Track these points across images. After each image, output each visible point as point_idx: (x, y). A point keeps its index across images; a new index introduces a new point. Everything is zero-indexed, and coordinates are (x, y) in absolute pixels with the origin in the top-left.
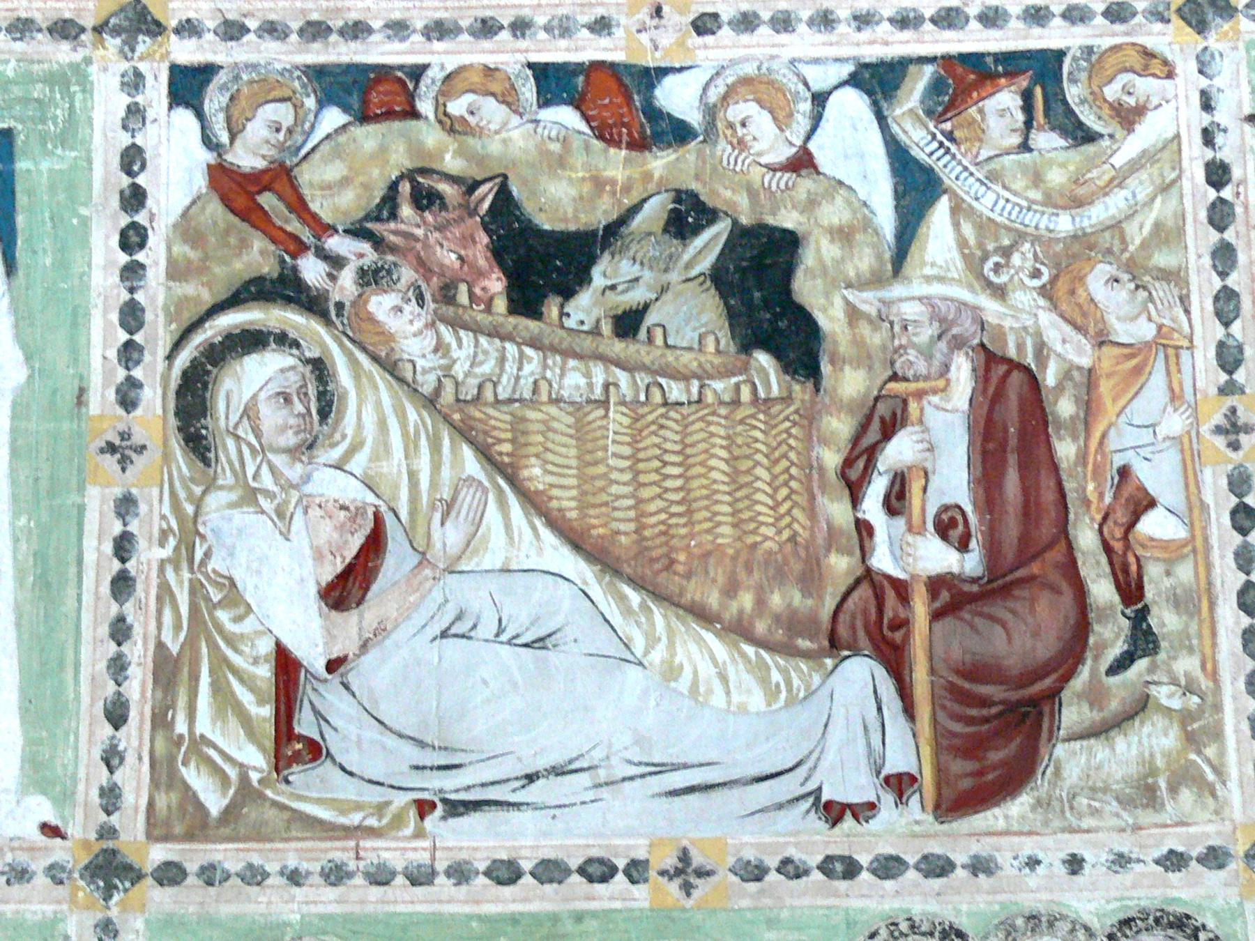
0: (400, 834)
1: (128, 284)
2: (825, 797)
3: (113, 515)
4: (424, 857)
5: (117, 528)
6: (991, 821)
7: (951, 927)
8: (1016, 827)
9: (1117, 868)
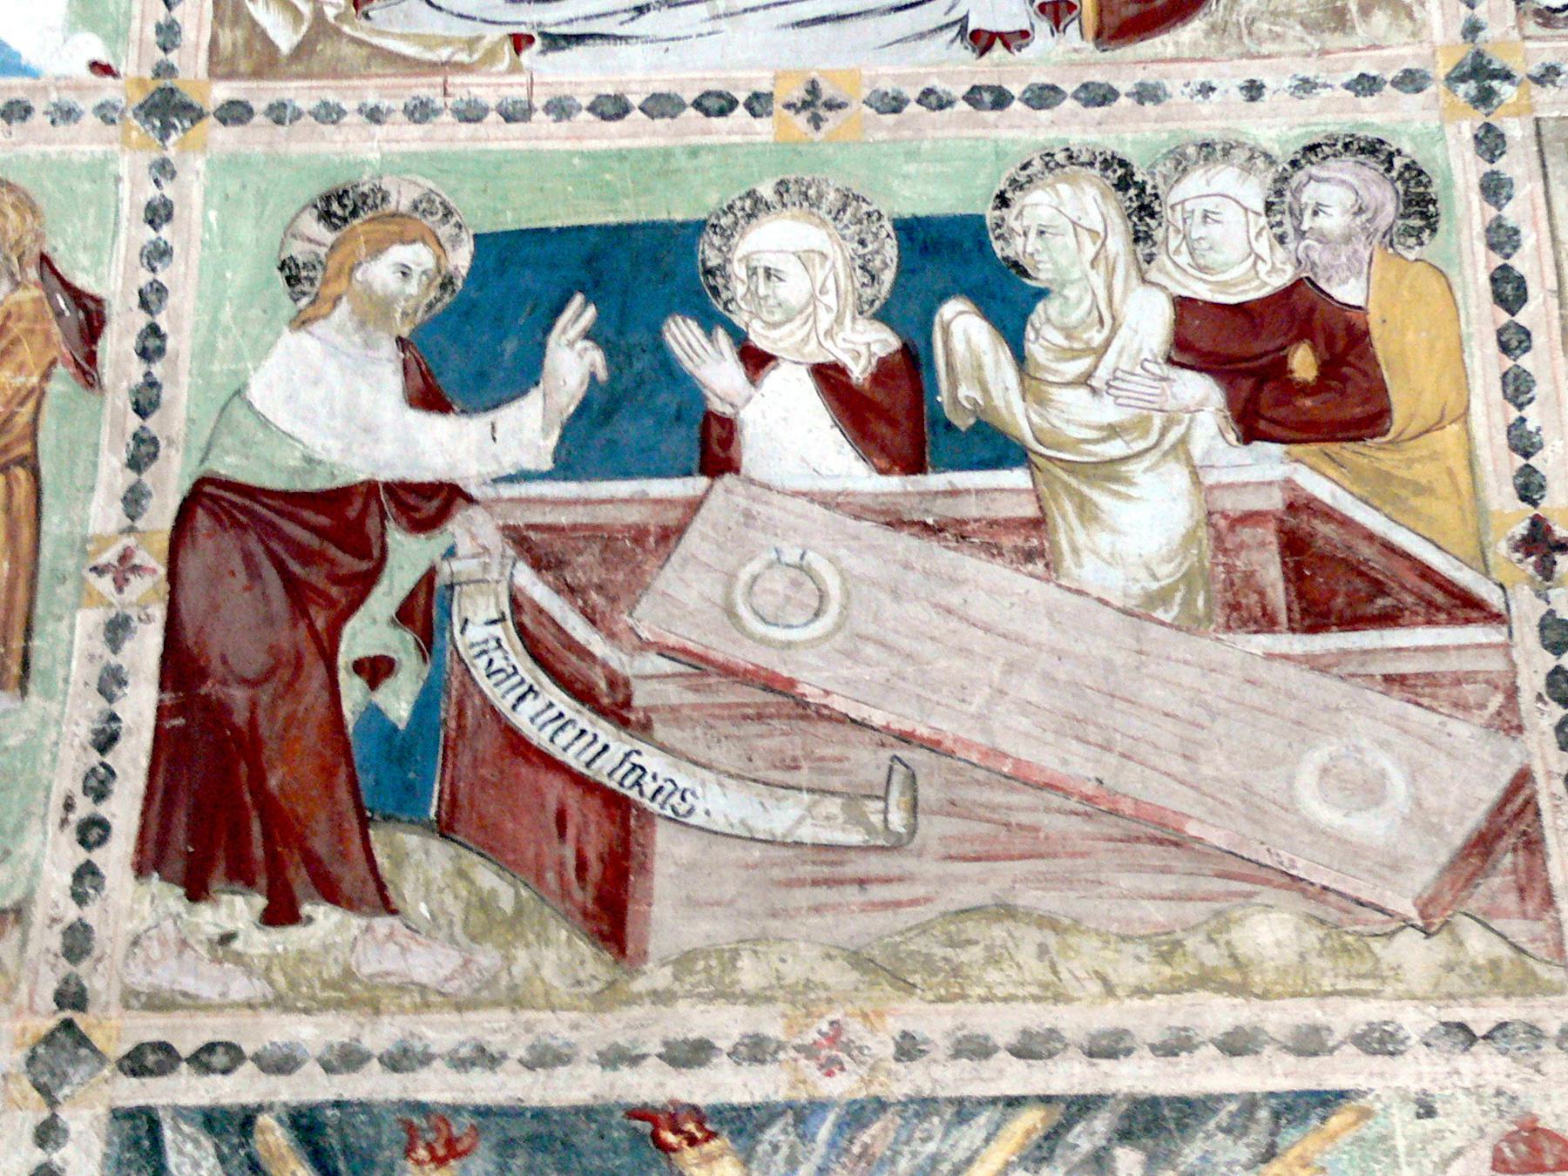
0: (494, 70)
2: (971, 27)
4: (520, 93)
6: (1160, 48)
7: (1113, 157)
8: (1187, 54)
9: (1301, 93)
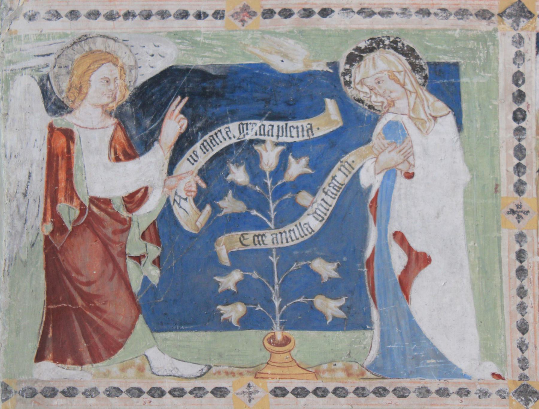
1: (518, 137)
3: (515, 242)
5: (517, 248)
